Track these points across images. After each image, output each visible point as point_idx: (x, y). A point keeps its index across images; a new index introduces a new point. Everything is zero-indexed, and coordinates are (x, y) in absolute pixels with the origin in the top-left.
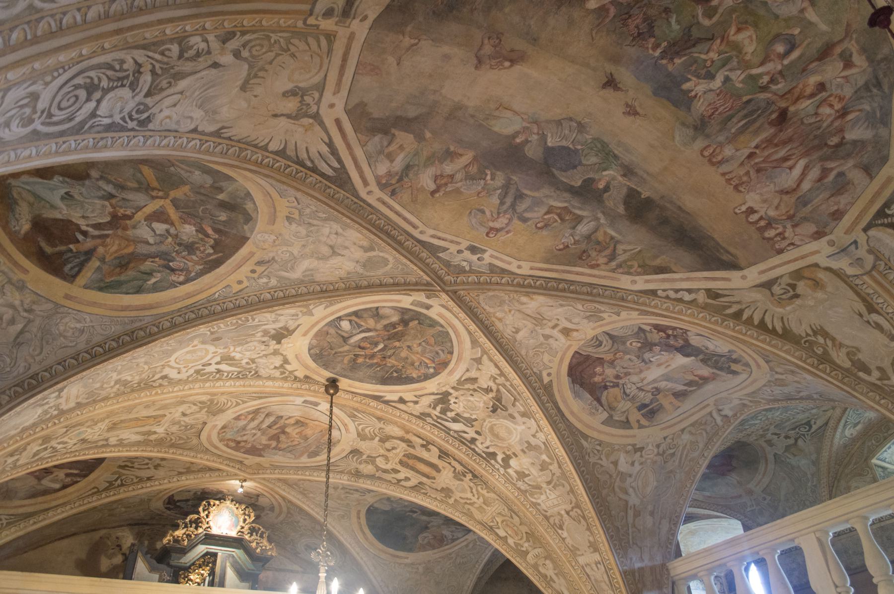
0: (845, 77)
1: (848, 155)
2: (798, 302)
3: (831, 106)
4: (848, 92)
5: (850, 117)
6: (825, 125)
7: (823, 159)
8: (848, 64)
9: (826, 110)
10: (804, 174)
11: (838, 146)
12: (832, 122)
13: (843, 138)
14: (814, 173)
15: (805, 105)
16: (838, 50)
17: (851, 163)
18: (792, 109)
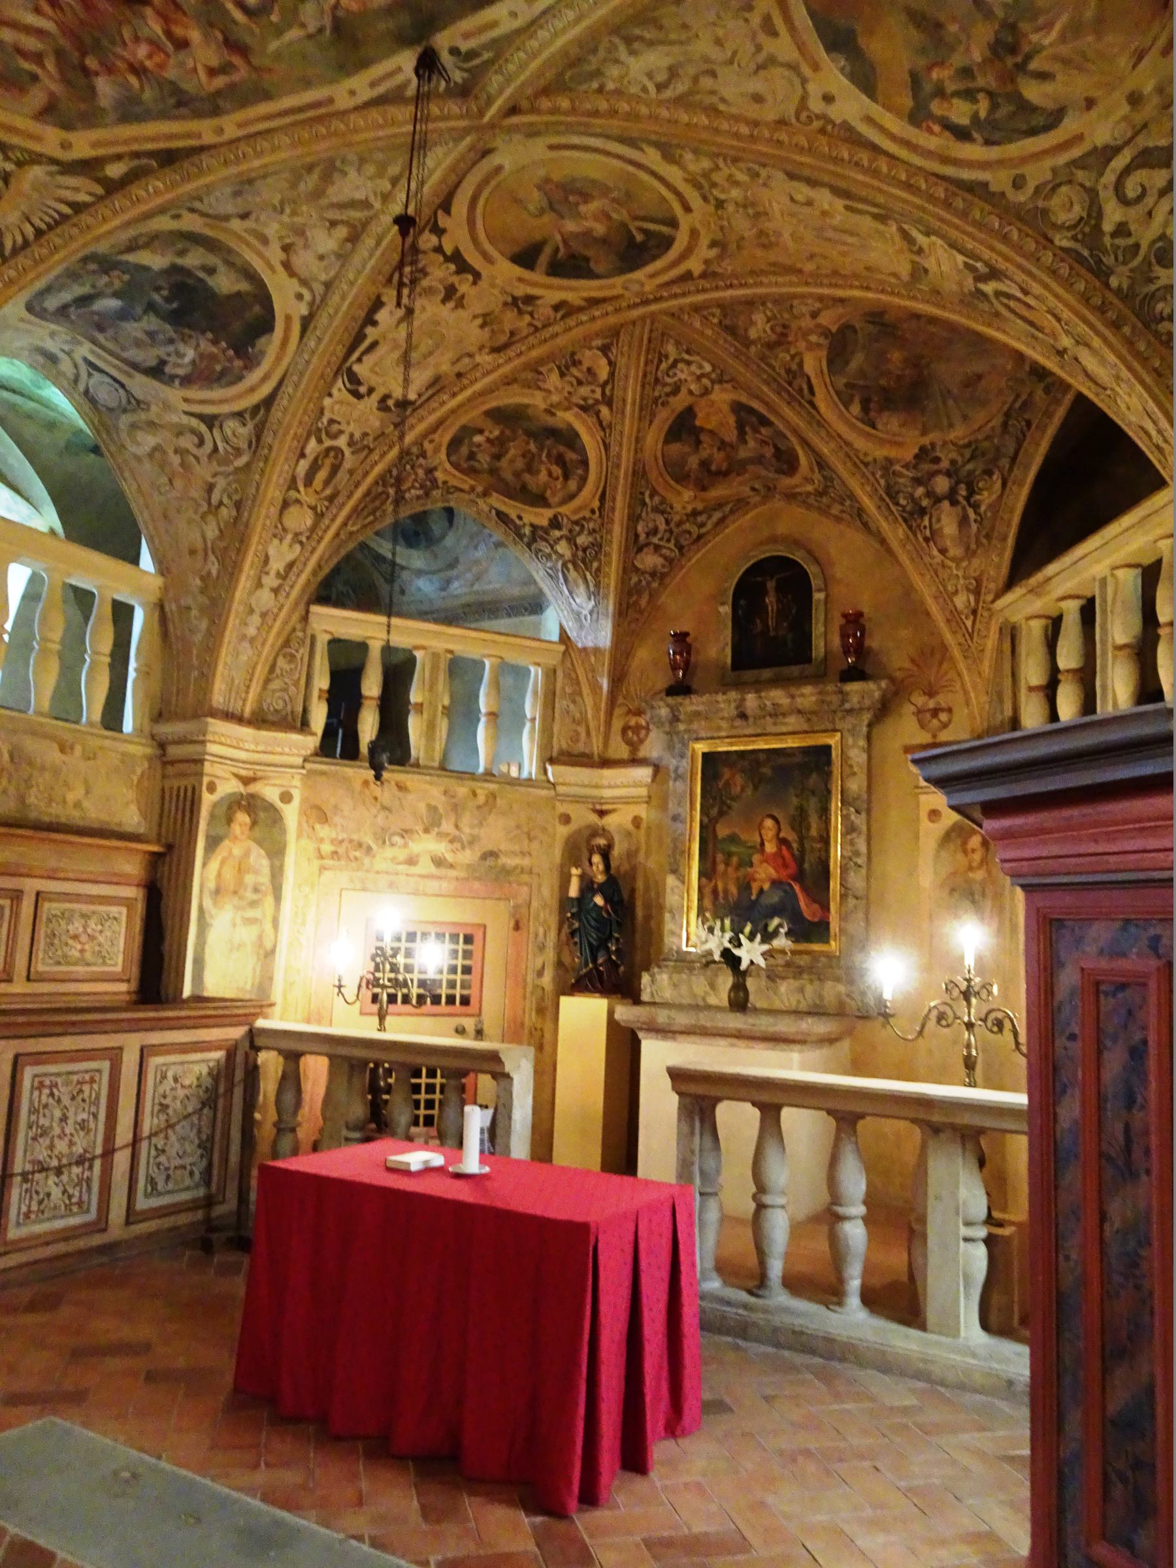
0: (195, 70)
1: (66, 81)
3: (150, 56)
4: (171, 73)
5: (133, 80)
6: (119, 50)
7: (59, 54)
8: (212, 72)
9: (142, 51)
10: (28, 30)
11: (86, 72)
12: (122, 58)
13: (97, 74)
14: (31, 43)
15: (155, 27)
16: (237, 60)
17: (55, 87)
18: (149, 12)
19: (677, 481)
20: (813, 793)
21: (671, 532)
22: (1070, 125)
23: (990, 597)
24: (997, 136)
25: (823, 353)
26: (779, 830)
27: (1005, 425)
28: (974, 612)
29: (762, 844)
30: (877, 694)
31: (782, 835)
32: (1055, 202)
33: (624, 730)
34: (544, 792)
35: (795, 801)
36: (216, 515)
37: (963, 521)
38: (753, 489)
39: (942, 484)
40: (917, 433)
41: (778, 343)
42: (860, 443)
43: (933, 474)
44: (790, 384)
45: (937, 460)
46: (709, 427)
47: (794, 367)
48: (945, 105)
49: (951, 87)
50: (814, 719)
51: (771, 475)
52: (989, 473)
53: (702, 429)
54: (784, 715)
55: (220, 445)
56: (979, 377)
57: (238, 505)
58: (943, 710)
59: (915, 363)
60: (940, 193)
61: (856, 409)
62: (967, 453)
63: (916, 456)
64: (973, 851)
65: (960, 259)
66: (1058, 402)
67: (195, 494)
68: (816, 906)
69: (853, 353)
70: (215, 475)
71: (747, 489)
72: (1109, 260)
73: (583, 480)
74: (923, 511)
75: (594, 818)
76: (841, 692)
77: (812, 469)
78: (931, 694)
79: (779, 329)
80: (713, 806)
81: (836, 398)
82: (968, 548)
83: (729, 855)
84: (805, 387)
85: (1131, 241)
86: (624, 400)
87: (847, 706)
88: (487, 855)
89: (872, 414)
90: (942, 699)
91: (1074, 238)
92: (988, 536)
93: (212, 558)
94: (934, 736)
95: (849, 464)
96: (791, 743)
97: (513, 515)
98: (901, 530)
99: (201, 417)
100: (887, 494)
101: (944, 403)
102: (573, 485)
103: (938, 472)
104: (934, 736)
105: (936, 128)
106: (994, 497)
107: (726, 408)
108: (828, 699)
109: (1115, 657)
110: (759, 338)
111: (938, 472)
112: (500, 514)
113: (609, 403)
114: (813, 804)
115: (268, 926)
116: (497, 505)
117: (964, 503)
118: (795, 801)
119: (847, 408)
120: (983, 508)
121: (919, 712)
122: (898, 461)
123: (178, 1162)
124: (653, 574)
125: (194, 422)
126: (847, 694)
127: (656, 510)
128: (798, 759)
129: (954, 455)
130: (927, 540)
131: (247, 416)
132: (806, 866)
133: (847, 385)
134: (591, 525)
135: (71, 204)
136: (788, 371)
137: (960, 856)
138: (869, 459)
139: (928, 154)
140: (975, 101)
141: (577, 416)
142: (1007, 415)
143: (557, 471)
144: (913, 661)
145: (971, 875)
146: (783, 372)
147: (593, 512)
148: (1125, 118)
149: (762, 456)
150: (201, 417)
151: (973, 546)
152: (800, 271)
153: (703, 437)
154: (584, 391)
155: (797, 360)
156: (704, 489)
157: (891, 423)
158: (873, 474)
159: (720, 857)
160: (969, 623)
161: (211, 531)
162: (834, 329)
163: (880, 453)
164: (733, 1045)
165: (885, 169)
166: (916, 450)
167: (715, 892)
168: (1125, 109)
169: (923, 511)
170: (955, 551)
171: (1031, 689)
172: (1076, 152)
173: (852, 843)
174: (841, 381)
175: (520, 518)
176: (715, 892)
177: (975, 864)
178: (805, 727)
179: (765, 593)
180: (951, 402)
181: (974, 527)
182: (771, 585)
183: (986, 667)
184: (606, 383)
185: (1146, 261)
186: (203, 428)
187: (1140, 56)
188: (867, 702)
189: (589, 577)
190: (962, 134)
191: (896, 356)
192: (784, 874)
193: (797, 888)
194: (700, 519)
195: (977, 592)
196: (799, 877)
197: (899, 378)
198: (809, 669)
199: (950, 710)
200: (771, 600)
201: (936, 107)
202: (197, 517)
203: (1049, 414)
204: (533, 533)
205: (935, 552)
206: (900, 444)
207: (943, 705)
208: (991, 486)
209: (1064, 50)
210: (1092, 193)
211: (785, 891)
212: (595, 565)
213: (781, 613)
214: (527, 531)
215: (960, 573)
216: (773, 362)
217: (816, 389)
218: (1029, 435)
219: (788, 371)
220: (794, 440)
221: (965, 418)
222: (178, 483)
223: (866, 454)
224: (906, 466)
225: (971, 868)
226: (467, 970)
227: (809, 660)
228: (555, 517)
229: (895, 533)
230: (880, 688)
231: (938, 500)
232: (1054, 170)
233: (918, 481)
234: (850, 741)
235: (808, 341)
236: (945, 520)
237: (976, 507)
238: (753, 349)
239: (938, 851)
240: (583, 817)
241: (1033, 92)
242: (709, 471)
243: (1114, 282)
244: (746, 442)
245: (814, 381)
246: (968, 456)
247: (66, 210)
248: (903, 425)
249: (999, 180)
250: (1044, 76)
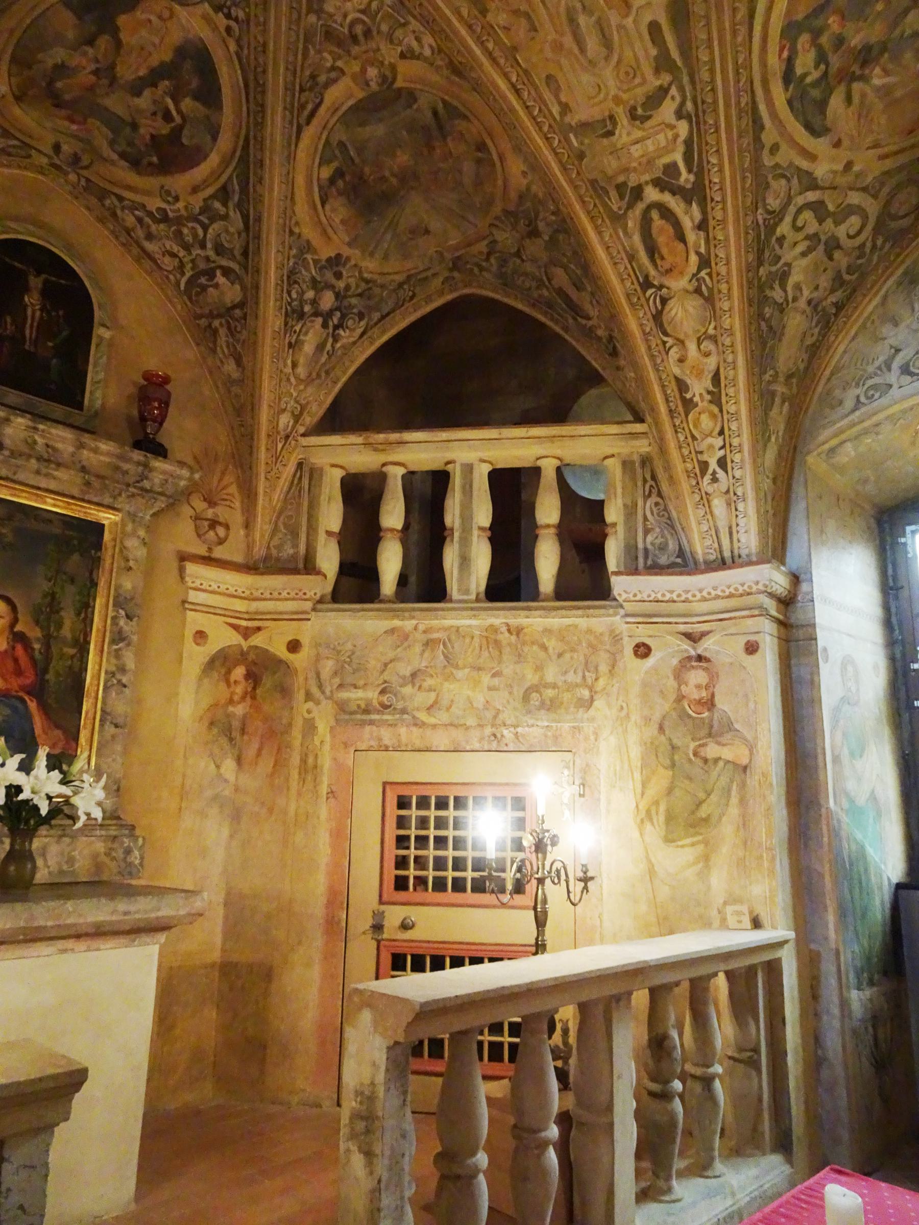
19: (14, 60)
20: (72, 581)
22: (819, 145)
23: (302, 430)
24: (797, 104)
25: (361, 95)
26: (15, 621)
27: (401, 285)
28: (287, 437)
30: (183, 483)
31: (18, 628)
35: (46, 586)
37: (320, 347)
38: (57, 148)
39: (328, 301)
40: (347, 239)
41: (340, 44)
42: (302, 209)
44: (302, 90)
45: (338, 276)
46: (123, 36)
47: (322, 79)
48: (807, 46)
49: (824, 40)
50: (96, 483)
51: (106, 151)
52: (361, 316)
53: (115, 32)
54: (59, 465)
56: (427, 232)
58: (220, 524)
59: (408, 178)
60: (744, 101)
61: (326, 173)
62: (363, 286)
63: (329, 260)
64: (235, 682)
65: (678, 157)
66: (441, 293)
68: (58, 733)
69: (381, 120)
71: (51, 139)
76: (146, 465)
77: (195, 190)
78: (212, 503)
79: (359, 29)
81: (320, 147)
82: (310, 374)
84: (310, 107)
87: (146, 484)
89: (334, 190)
90: (221, 512)
92: (327, 373)
94: (210, 550)
95: (281, 221)
96: (50, 505)
98: (279, 323)
100: (289, 277)
101: (384, 233)
103: (332, 287)
104: (210, 550)
105: (785, 54)
106: (352, 340)
107: (176, 37)
108: (126, 466)
109: (479, 536)
110: (331, 16)
111: (332, 287)
114: (69, 597)
117: (331, 330)
118: (46, 586)
119: (320, 165)
120: (338, 345)
121: (197, 518)
122: (315, 252)
126: (151, 470)
128: (57, 530)
129: (352, 281)
130: (290, 345)
132: (50, 676)
133: (342, 144)
136: (313, 77)
137: (222, 685)
138: (297, 230)
139: (764, 64)
140: (816, 67)
144: (195, 458)
145: (231, 709)
146: (307, 73)
148: (835, 172)
149: (135, 126)
151: (314, 375)
152: (484, 12)
153: (103, 42)
155: (333, 75)
156: (18, 99)
158: (290, 248)
160: (280, 446)
162: (399, 84)
163: (308, 232)
164: (64, 951)
165: (740, 39)
166: (333, 255)
168: (840, 167)
169: (301, 315)
170: (301, 371)
171: (329, 533)
172: (804, 164)
173: (117, 654)
174: (341, 135)
177: (236, 698)
178: (76, 492)
179: (26, 289)
180: (388, 236)
181: (324, 358)
182: (36, 282)
183: (277, 496)
187: (876, 146)
188: (170, 490)
190: (788, 77)
191: (403, 158)
192: (15, 684)
193: (33, 705)
195: (297, 418)
196: (38, 691)
197: (383, 179)
198: (78, 418)
199: (227, 527)
200: (32, 301)
201: (804, 39)
203: (429, 299)
205: (289, 362)
207: (221, 520)
208: (354, 330)
209: (871, 96)
210: (790, 199)
211: (15, 710)
213: (45, 329)
215: (295, 394)
216: (312, 52)
217: (315, 121)
218: (407, 305)
219: (313, 77)
220: (225, 142)
221: (386, 257)
223: (297, 224)
224: (314, 260)
225: (231, 701)
226: (458, 885)
227: (80, 406)
230: (190, 479)
231: (316, 314)
232: (791, 164)
233: (314, 284)
234: (129, 527)
235: (364, 71)
236: (310, 335)
237: (336, 339)
238: (312, 18)
239: (200, 679)
241: (836, 102)
242: (51, 83)
244: (139, 94)
245: (322, 110)
246: (360, 291)
249: (769, 136)
250: (849, 99)
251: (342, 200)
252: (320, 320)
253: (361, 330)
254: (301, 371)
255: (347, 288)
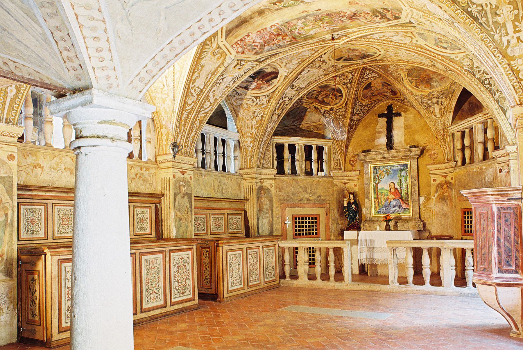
2: (213, 57)
21: (362, 110)
24: (452, 49)
27: (450, 87)
29: (390, 190)
32: (464, 61)
33: (350, 161)
34: (331, 179)
36: (256, 119)
42: (414, 91)
43: (432, 98)
55: (258, 102)
57: (262, 116)
61: (414, 84)
62: (441, 93)
67: (249, 114)
70: (256, 109)
72: (475, 72)
73: (341, 99)
74: (430, 107)
75: (343, 185)
80: (376, 181)
83: (382, 193)
85: (480, 69)
86: (355, 83)
88: (318, 197)
91: (468, 68)
93: (254, 129)
97: (319, 107)
99: (254, 97)
102: (337, 101)
112: (315, 107)
113: (351, 83)
115: (271, 219)
116: (315, 105)
123: (269, 272)
124: (357, 120)
125: (252, 98)
127: (359, 105)
131: (266, 96)
134: (342, 110)
135: (252, 67)
141: (341, 86)
142: (451, 85)
143: (334, 97)
147: (343, 107)
150: (254, 97)
151: (443, 114)
154: (345, 81)
157: (422, 87)
159: (379, 193)
161: (254, 122)
167: (378, 202)
170: (438, 116)
175: (321, 108)
176: (378, 202)
184: (350, 79)
185: (483, 73)
186: (255, 99)
189: (340, 123)
194: (369, 106)
199: (437, 154)
202: (250, 119)
204: (325, 112)
205: (433, 116)
206: (425, 92)
212: (343, 120)
214: (323, 111)
217: (404, 80)
221: (441, 86)
222: (246, 111)
228: (332, 108)
229: (423, 112)
231: (434, 104)
240: (340, 185)
243: (476, 76)
247: (251, 68)
248: (425, 87)
249: (453, 56)
251: (421, 85)
252: (436, 105)
253: (448, 101)
254: (438, 116)
255: (438, 95)
